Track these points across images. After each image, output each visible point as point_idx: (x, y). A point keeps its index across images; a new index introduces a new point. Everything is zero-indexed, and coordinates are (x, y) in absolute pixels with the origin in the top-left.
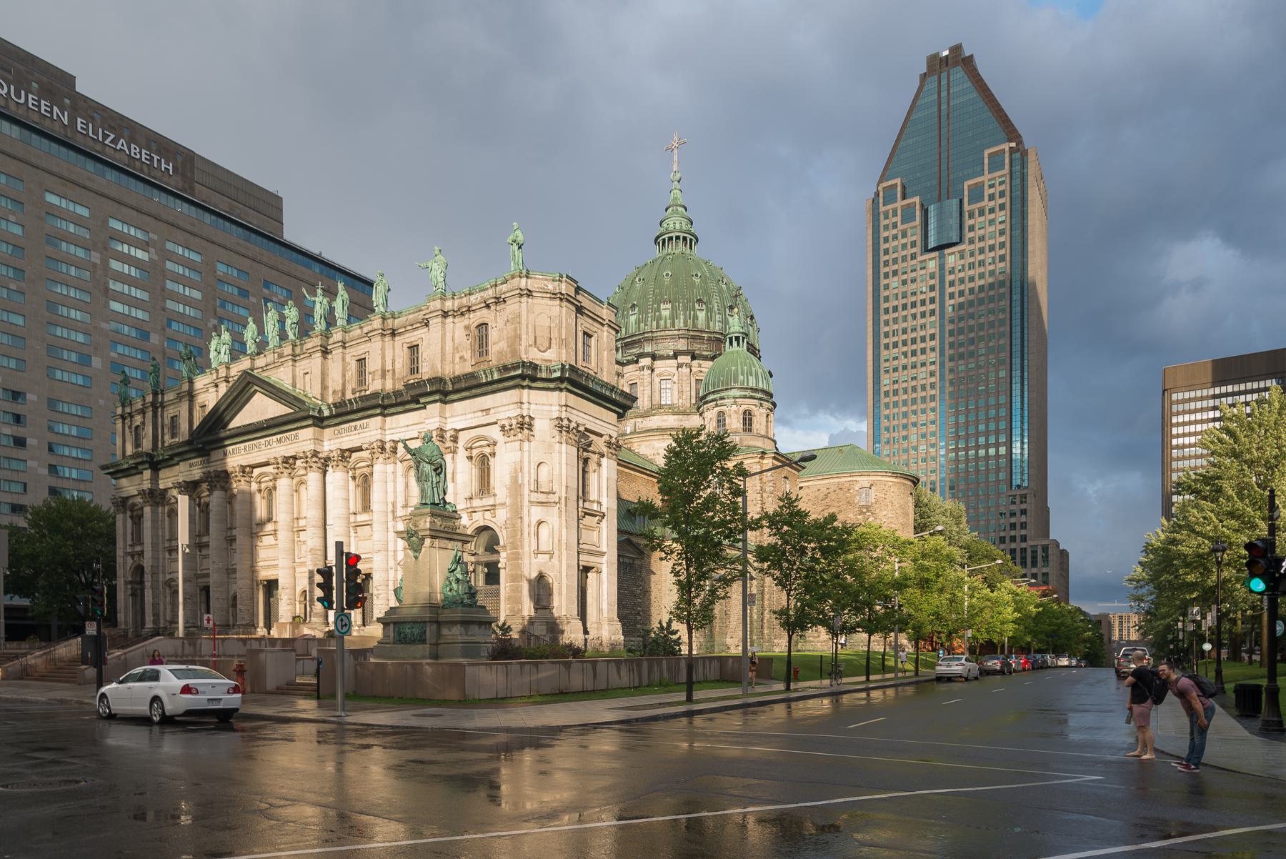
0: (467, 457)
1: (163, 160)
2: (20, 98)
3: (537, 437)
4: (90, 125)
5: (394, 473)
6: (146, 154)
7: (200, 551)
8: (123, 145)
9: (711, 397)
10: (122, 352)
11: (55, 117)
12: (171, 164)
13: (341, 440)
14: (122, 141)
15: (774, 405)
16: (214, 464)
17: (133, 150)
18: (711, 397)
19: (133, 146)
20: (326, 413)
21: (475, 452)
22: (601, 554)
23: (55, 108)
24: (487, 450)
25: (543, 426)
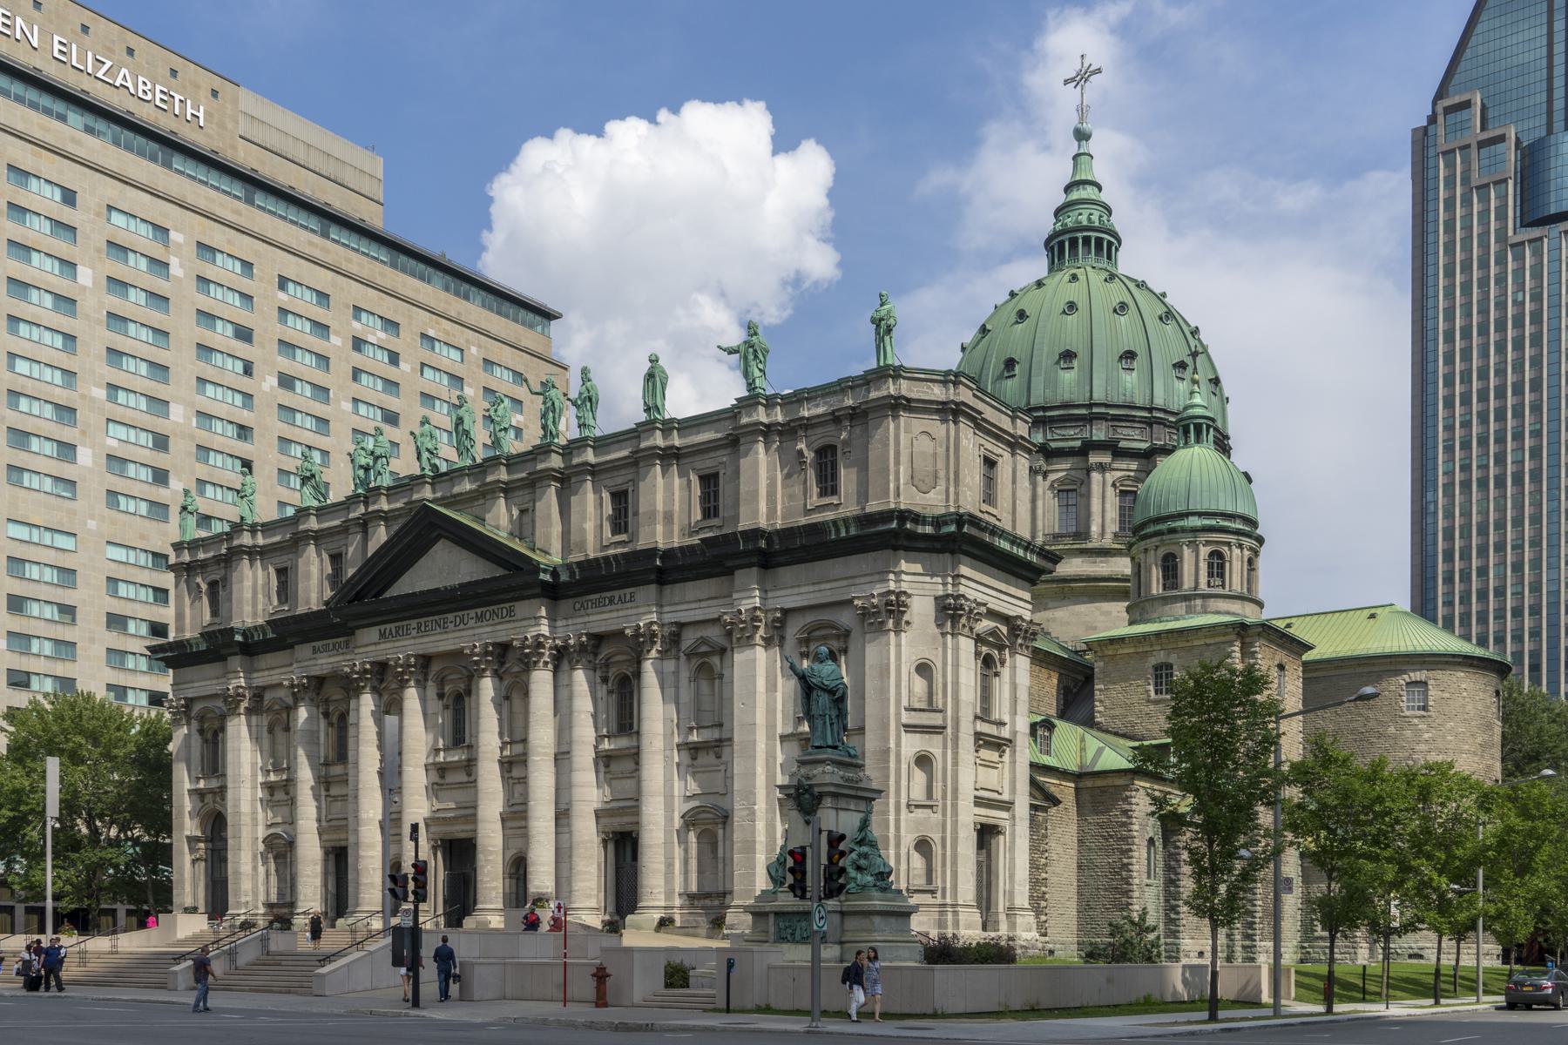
3: (914, 626)
5: (676, 673)
7: (327, 790)
9: (1151, 529)
10: (124, 438)
13: (586, 619)
15: (1260, 540)
16: (361, 650)
18: (1151, 529)
20: (564, 577)
22: (1007, 806)
25: (921, 609)
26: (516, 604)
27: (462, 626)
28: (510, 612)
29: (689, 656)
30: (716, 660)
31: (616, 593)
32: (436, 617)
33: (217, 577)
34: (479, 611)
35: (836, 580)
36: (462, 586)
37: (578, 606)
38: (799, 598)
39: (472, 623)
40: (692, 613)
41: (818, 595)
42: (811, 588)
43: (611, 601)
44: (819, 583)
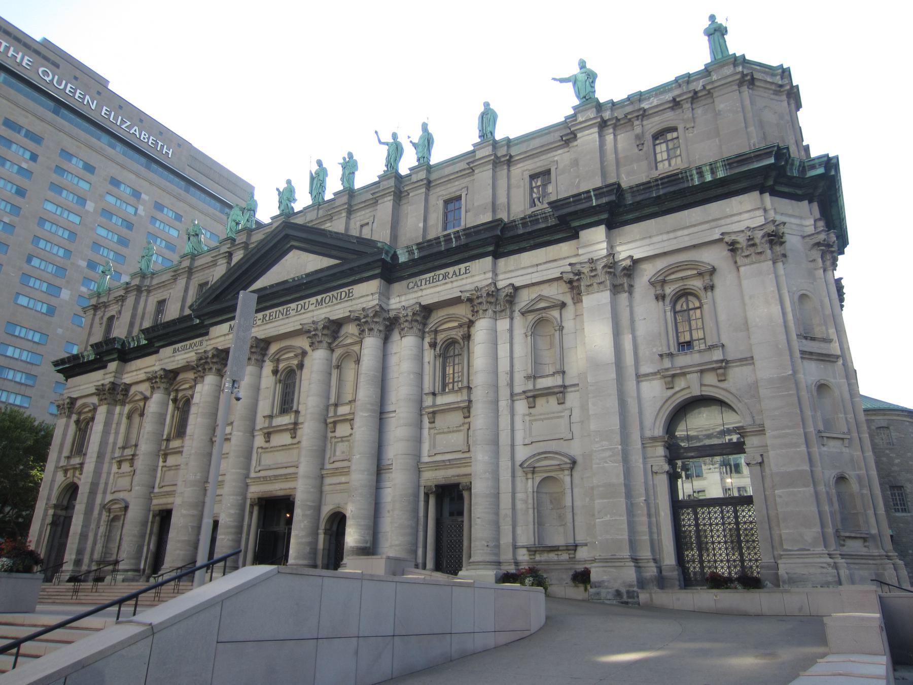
0: (657, 298)
1: (165, 146)
2: (60, 85)
4: (113, 113)
5: (511, 330)
6: (153, 140)
8: (135, 131)
11: (85, 103)
12: (171, 150)
13: (420, 294)
14: (136, 128)
17: (143, 136)
19: (143, 133)
21: (669, 290)
23: (87, 97)
24: (697, 284)
26: (355, 287)
27: (303, 311)
28: (348, 294)
29: (523, 314)
30: (555, 313)
31: (450, 270)
32: (281, 308)
33: (113, 313)
34: (319, 298)
35: (695, 226)
36: (308, 275)
37: (411, 285)
38: (652, 247)
39: (312, 307)
40: (529, 277)
41: (675, 241)
42: (665, 237)
43: (445, 277)
44: (674, 231)
